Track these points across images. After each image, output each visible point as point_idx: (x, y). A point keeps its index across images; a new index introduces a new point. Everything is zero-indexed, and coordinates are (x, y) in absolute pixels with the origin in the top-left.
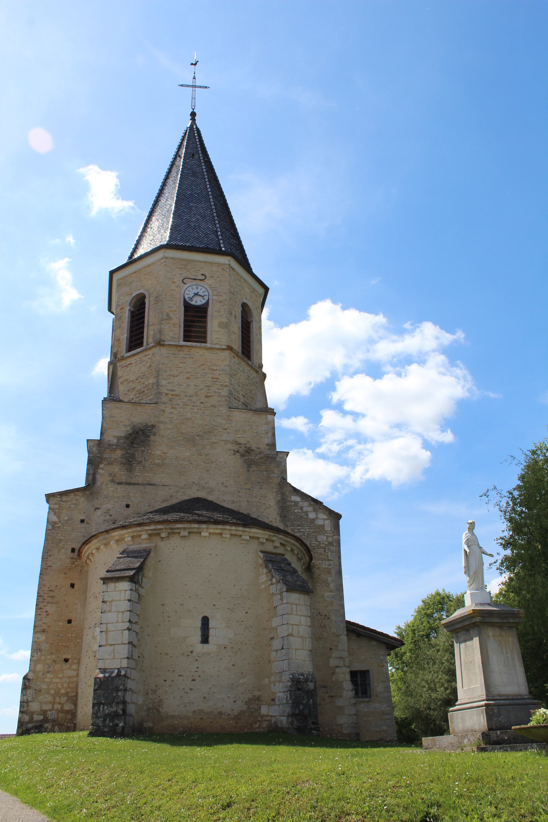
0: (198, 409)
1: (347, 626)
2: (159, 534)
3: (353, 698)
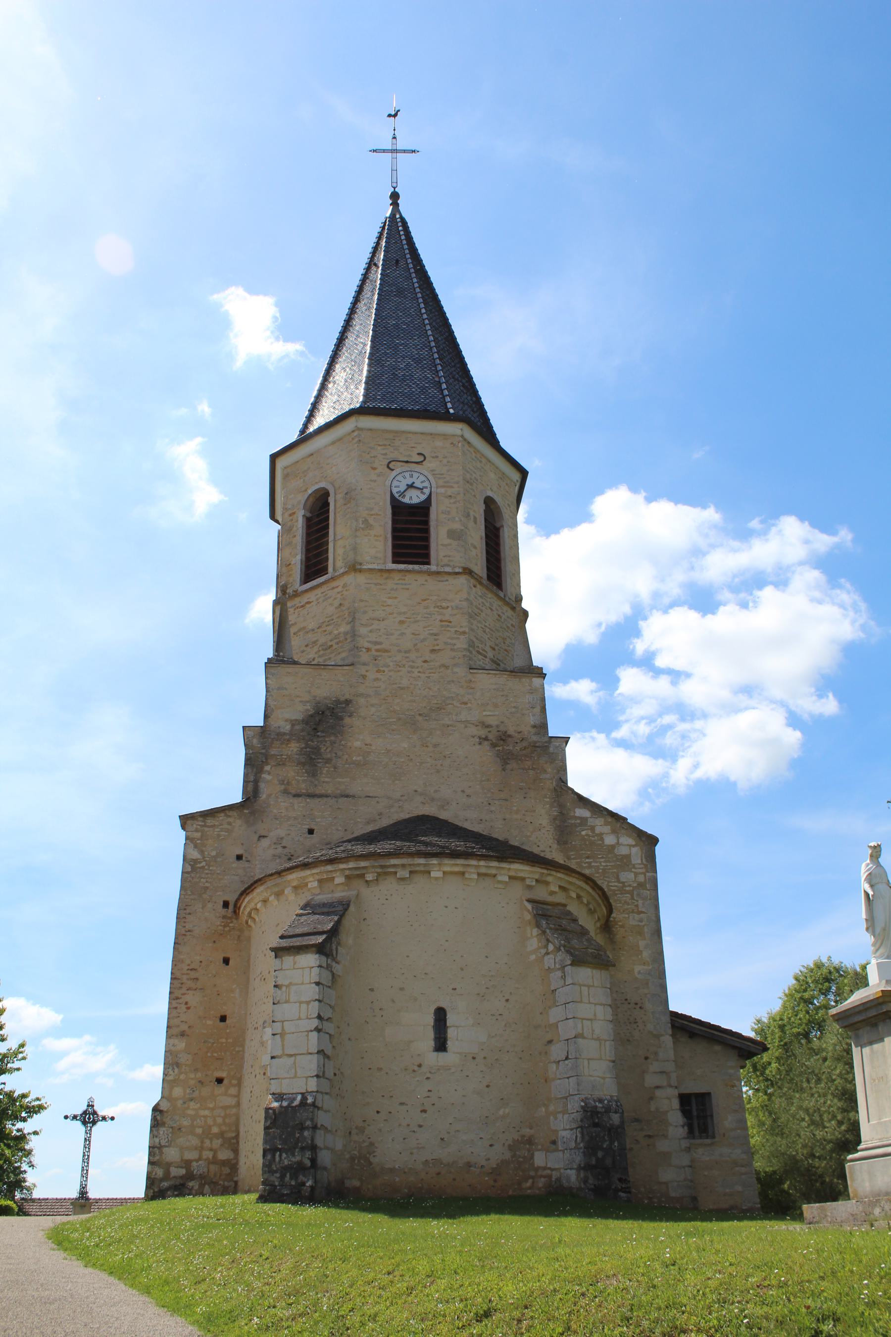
0: (419, 672)
1: (671, 1020)
2: (362, 876)
3: (684, 1138)
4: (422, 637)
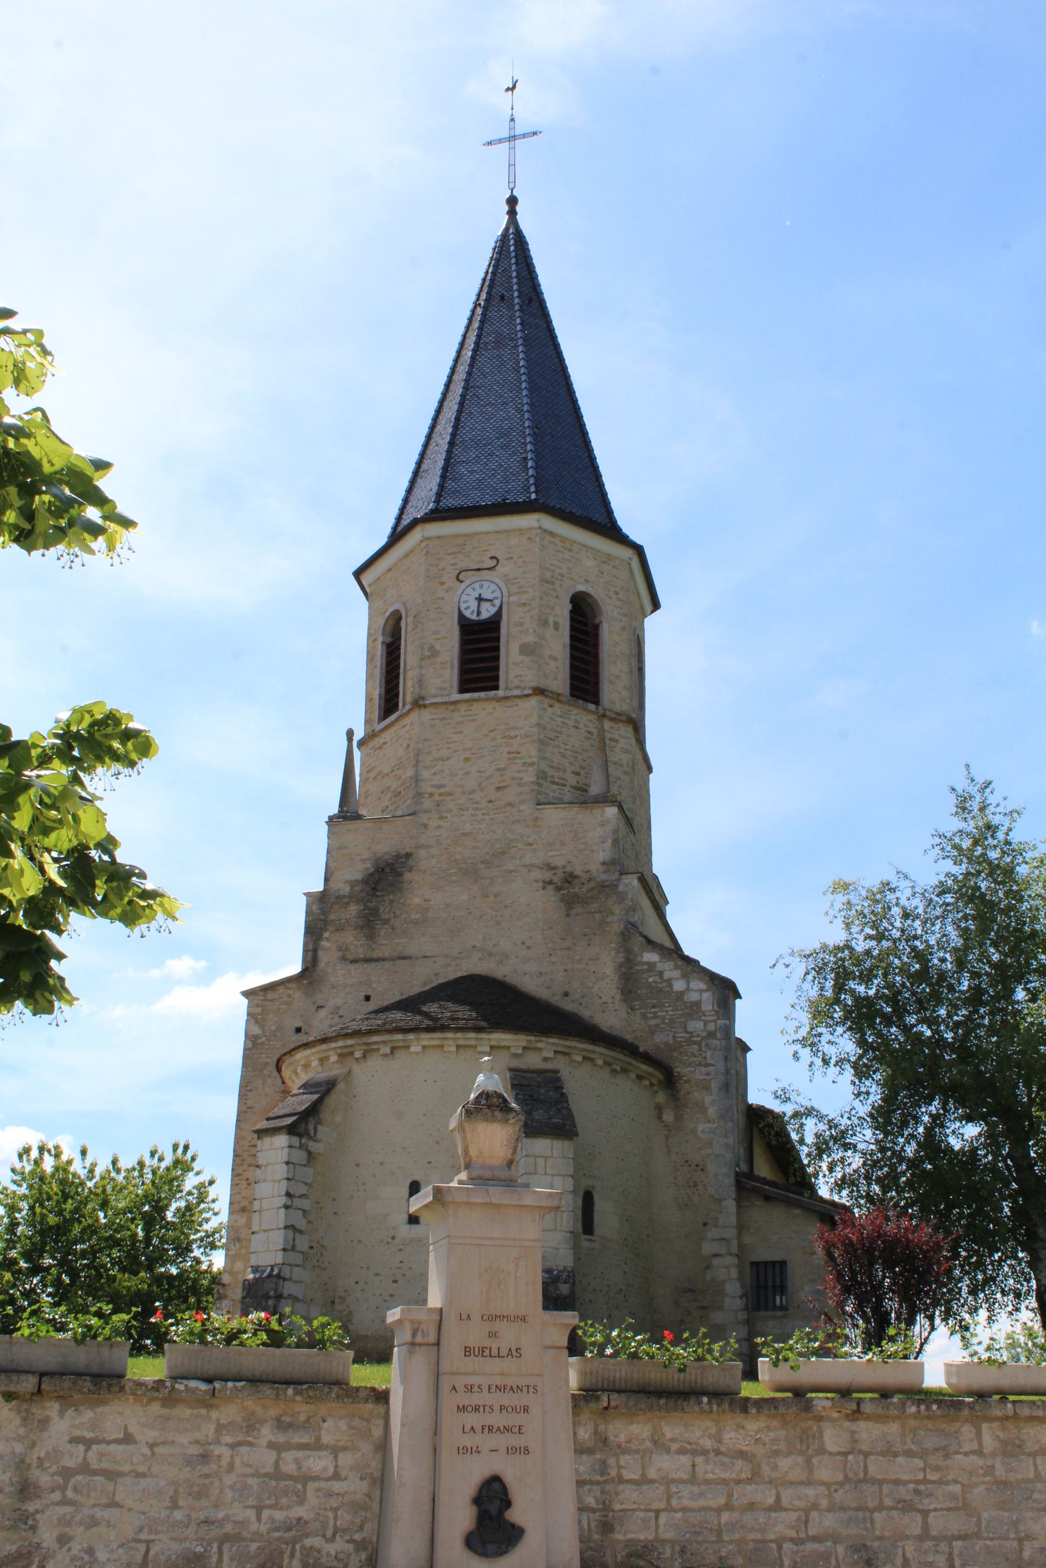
2: (352, 1054)
4: (487, 774)
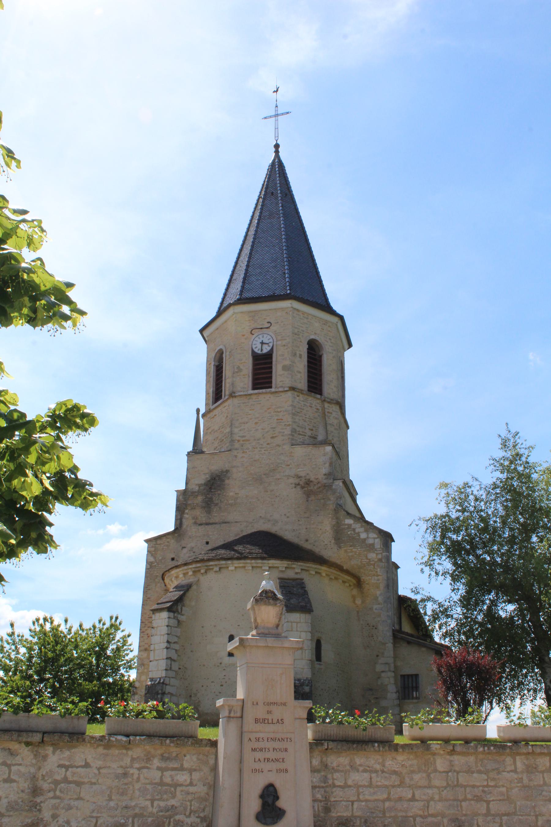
0: (265, 450)
2: (199, 571)
